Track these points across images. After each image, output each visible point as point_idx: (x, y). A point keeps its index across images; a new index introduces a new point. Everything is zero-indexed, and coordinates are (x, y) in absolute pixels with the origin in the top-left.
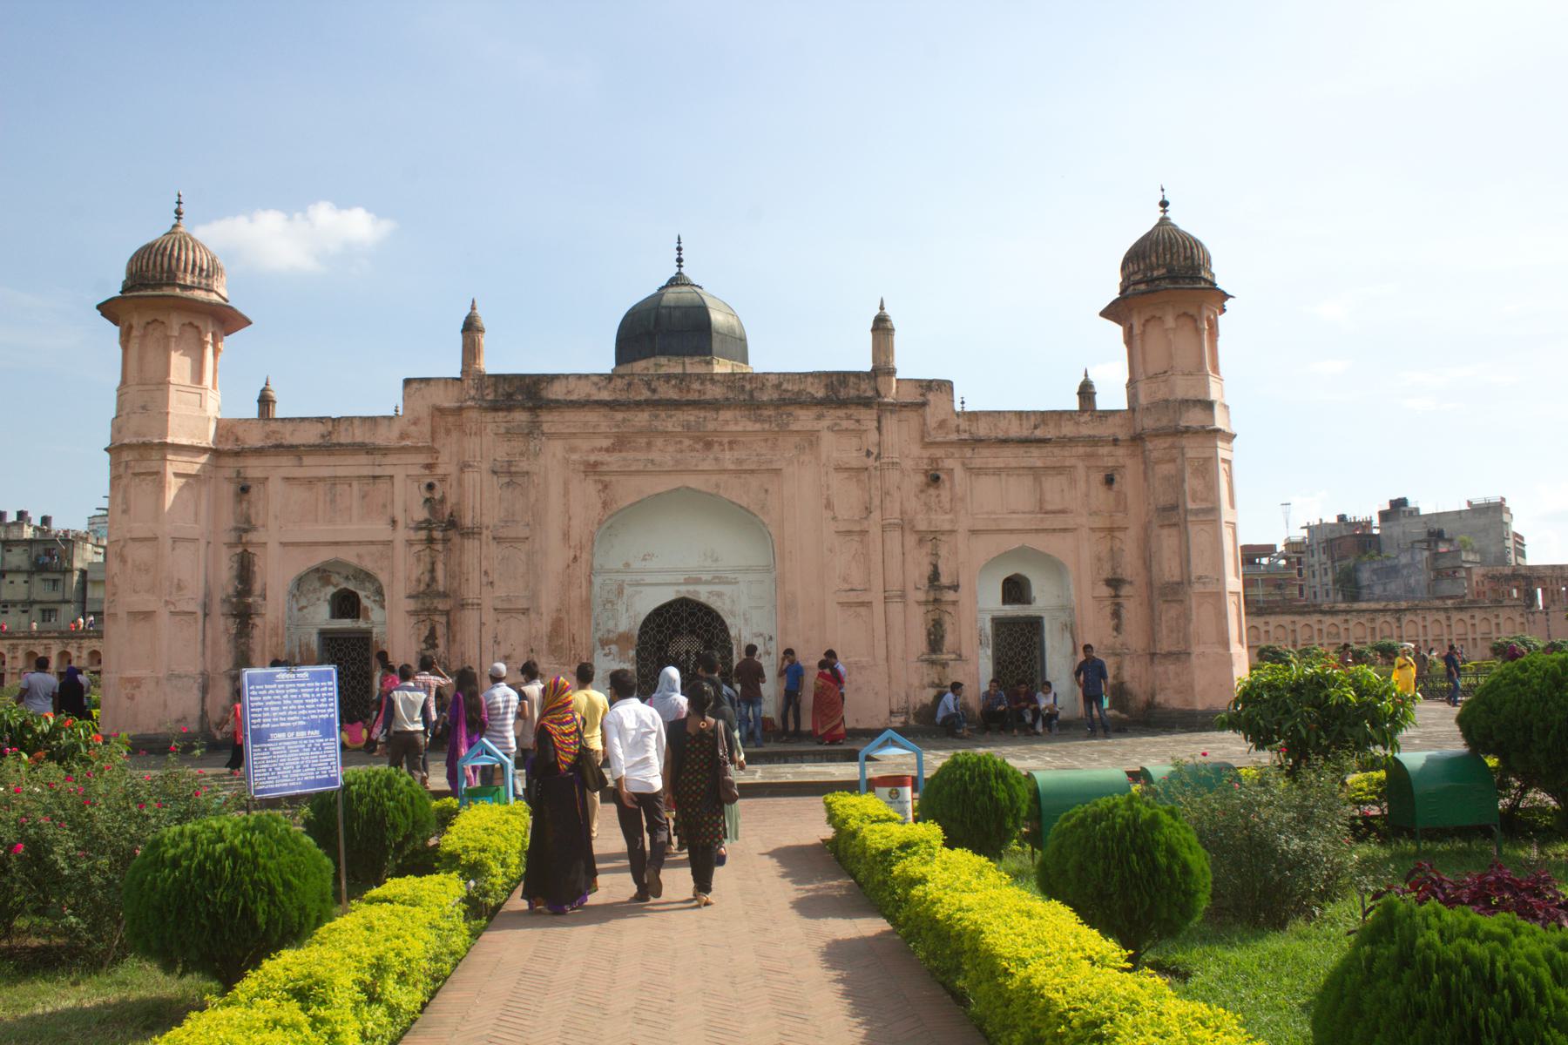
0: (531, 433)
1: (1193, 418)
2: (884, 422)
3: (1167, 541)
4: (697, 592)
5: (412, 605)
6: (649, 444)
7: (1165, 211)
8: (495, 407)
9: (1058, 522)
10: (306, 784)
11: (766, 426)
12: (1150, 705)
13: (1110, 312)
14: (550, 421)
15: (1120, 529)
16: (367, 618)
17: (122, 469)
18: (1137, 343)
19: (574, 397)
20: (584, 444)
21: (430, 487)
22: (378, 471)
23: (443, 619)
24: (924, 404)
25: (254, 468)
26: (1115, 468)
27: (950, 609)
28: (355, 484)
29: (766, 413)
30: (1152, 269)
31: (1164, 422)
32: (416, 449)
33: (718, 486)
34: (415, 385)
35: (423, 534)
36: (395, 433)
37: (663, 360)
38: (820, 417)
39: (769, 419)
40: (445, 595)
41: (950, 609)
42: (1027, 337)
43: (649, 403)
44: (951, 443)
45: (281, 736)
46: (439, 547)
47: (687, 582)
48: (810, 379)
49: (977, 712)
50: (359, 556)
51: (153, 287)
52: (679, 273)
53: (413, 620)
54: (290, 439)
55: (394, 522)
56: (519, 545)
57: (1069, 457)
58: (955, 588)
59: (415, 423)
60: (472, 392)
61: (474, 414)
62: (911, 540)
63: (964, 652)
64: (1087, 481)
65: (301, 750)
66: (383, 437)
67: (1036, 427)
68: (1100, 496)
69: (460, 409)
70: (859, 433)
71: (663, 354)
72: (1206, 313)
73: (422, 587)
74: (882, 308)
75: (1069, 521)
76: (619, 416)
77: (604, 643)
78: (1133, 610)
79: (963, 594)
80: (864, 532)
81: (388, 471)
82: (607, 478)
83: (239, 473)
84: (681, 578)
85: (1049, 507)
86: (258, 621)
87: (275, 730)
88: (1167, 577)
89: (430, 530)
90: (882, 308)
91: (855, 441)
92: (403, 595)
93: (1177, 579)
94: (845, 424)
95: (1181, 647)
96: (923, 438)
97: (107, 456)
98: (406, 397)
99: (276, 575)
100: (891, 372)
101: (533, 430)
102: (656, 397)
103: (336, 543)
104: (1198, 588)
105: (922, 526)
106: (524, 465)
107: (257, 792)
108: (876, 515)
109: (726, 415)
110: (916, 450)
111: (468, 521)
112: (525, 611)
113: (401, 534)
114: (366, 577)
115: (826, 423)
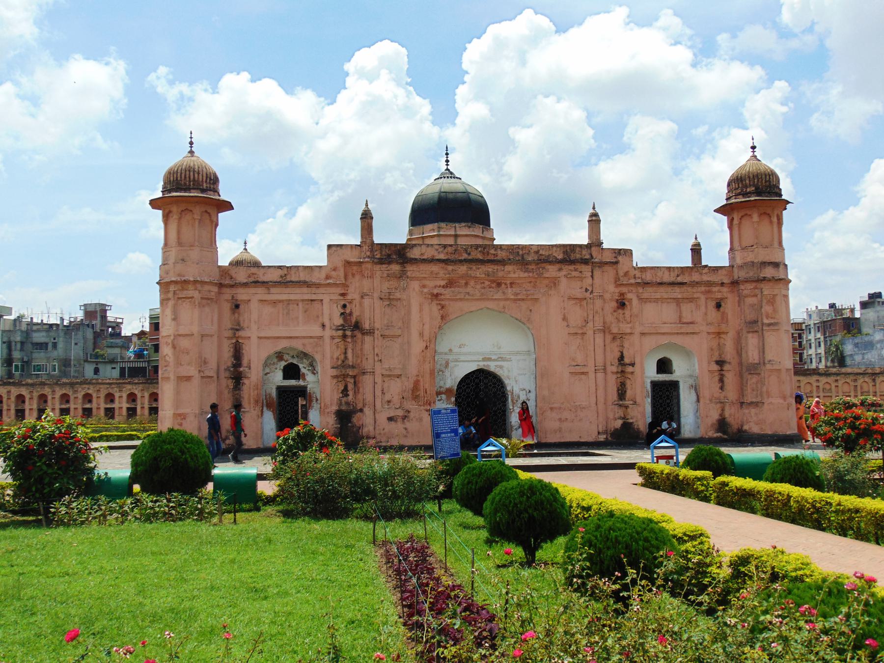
0: (401, 277)
1: (769, 272)
2: (595, 272)
3: (752, 341)
4: (488, 366)
5: (335, 372)
6: (466, 284)
7: (754, 152)
8: (381, 262)
9: (690, 328)
11: (531, 274)
12: (740, 431)
13: (721, 210)
14: (411, 269)
15: (723, 333)
16: (304, 379)
17: (170, 295)
18: (736, 229)
19: (425, 257)
20: (430, 284)
21: (344, 306)
22: (314, 297)
23: (352, 381)
24: (617, 263)
25: (242, 294)
26: (722, 299)
27: (630, 376)
28: (300, 304)
29: (530, 267)
30: (746, 187)
31: (751, 274)
32: (335, 285)
33: (504, 308)
34: (334, 249)
35: (340, 333)
36: (323, 276)
37: (443, 225)
38: (560, 270)
39: (532, 271)
40: (353, 367)
41: (630, 376)
42: (667, 219)
43: (466, 261)
44: (631, 284)
45: (443, 435)
46: (349, 340)
47: (484, 360)
48: (555, 249)
49: (645, 434)
50: (304, 345)
51: (185, 190)
52: (447, 169)
53: (335, 381)
54: (262, 278)
55: (323, 326)
56: (395, 339)
57: (697, 292)
58: (633, 365)
59: (334, 270)
60: (368, 253)
61: (369, 266)
62: (609, 338)
63: (638, 400)
64: (706, 307)
66: (316, 278)
67: (678, 276)
68: (713, 314)
69: (360, 263)
70: (581, 279)
71: (443, 221)
72: (776, 213)
73: (340, 362)
74: (594, 208)
75: (695, 328)
76: (450, 268)
77: (438, 393)
78: (730, 378)
79: (637, 368)
80: (584, 334)
81: (320, 297)
82: (443, 303)
83: (233, 297)
84: (481, 358)
85: (685, 321)
86: (246, 381)
88: (750, 361)
89: (345, 330)
90: (594, 208)
91: (579, 284)
92: (329, 367)
93: (756, 361)
94: (574, 274)
95: (759, 399)
96: (616, 282)
97: (158, 287)
98: (329, 256)
99: (256, 354)
100: (601, 244)
101: (402, 275)
102: (470, 258)
103: (291, 337)
104: (768, 366)
105: (615, 330)
106: (398, 295)
108: (590, 324)
109: (509, 268)
110: (612, 288)
111: (367, 326)
112: (399, 376)
113: (328, 333)
114: (305, 355)
115: (563, 273)
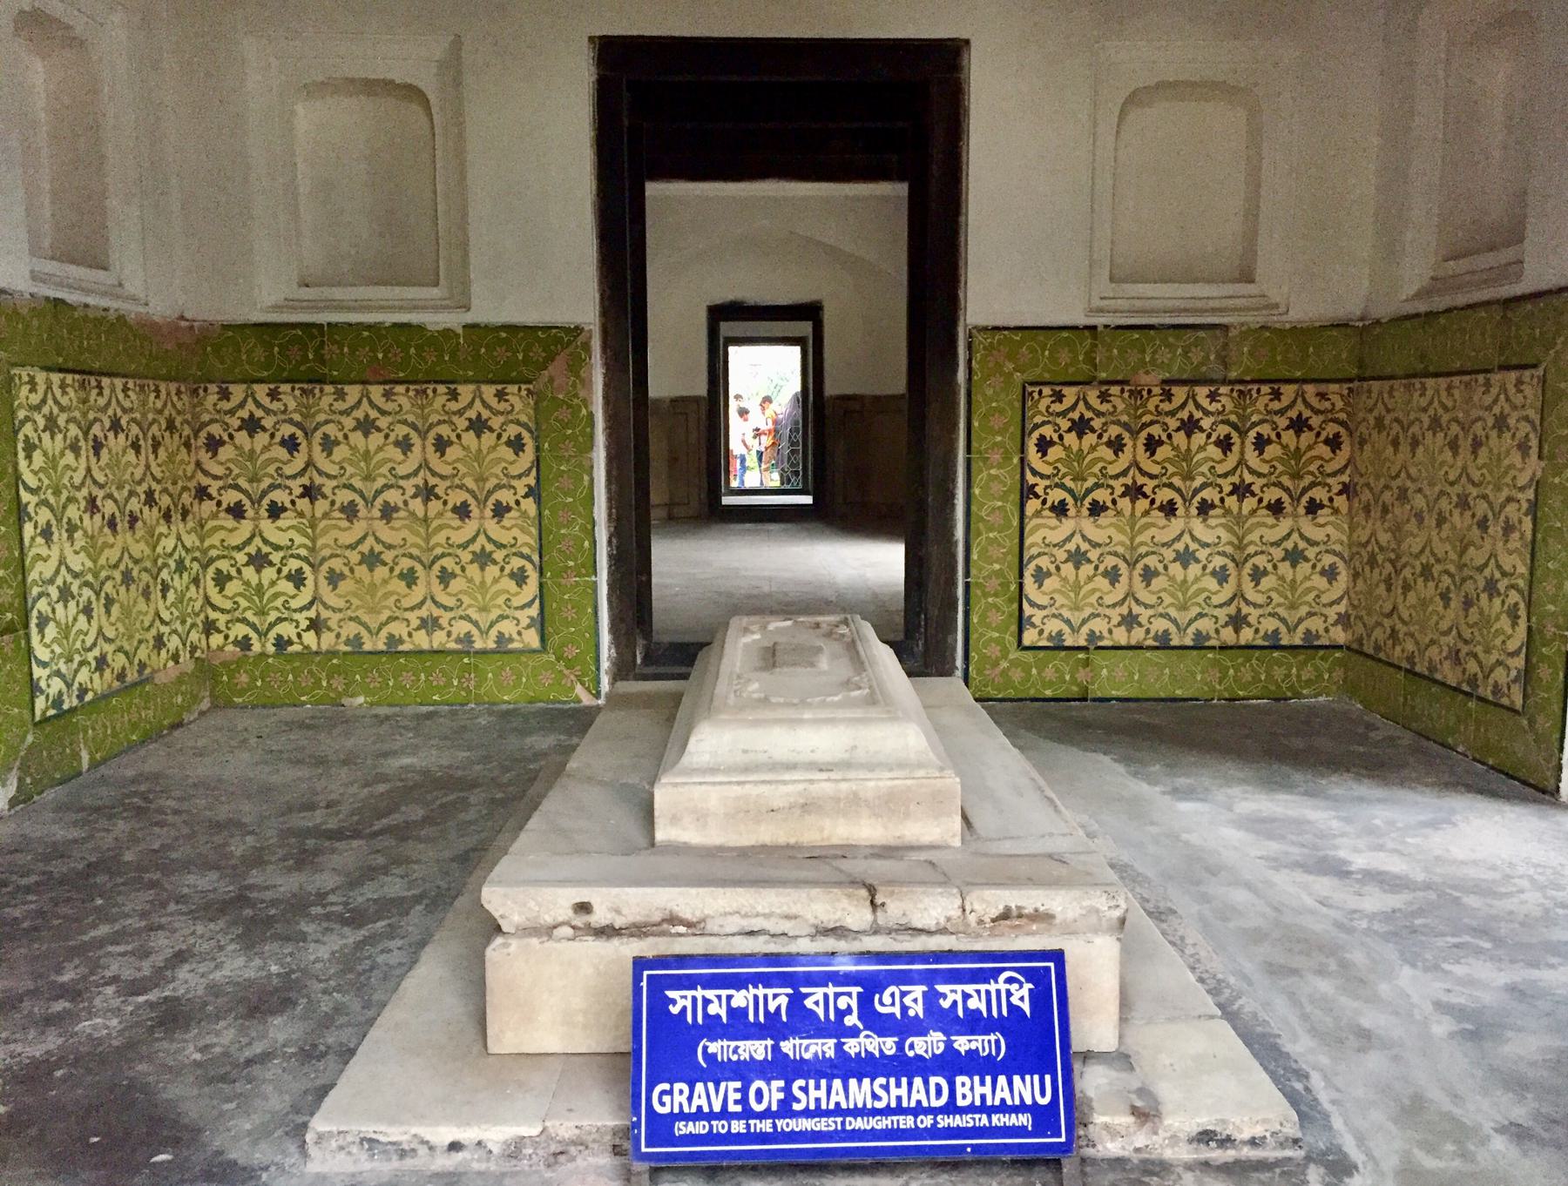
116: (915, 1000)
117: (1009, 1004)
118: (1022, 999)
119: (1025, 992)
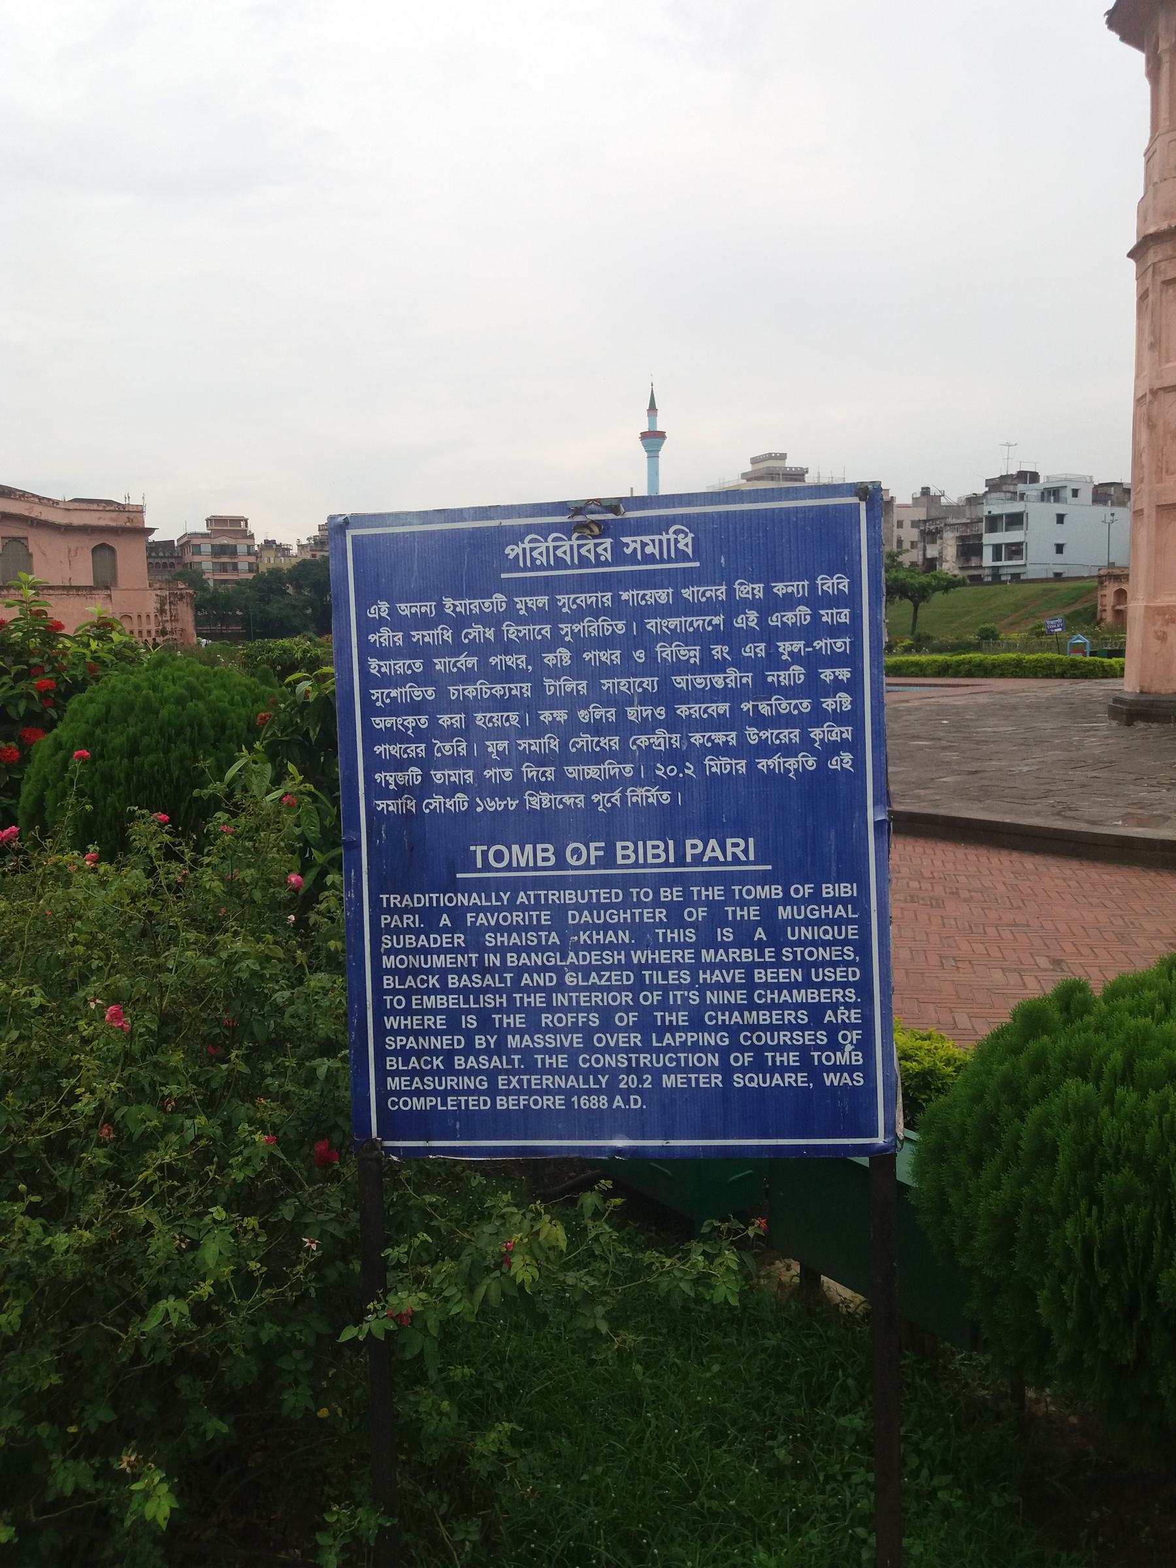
10: (666, 1111)
65: (642, 936)
87: (499, 829)
97: (1132, 263)
107: (393, 1124)
116: (605, 550)
117: (676, 548)
118: (686, 545)
119: (689, 540)
